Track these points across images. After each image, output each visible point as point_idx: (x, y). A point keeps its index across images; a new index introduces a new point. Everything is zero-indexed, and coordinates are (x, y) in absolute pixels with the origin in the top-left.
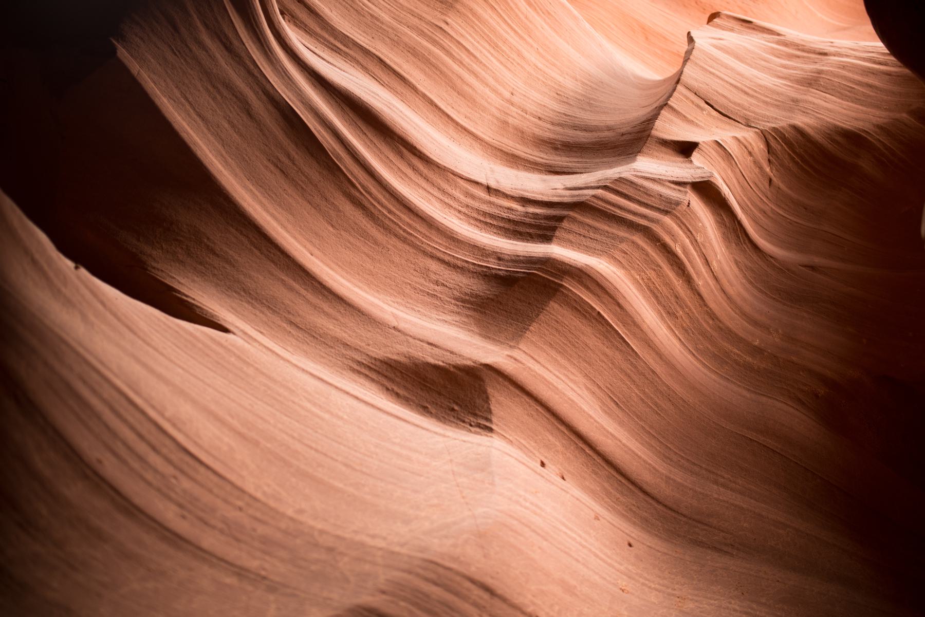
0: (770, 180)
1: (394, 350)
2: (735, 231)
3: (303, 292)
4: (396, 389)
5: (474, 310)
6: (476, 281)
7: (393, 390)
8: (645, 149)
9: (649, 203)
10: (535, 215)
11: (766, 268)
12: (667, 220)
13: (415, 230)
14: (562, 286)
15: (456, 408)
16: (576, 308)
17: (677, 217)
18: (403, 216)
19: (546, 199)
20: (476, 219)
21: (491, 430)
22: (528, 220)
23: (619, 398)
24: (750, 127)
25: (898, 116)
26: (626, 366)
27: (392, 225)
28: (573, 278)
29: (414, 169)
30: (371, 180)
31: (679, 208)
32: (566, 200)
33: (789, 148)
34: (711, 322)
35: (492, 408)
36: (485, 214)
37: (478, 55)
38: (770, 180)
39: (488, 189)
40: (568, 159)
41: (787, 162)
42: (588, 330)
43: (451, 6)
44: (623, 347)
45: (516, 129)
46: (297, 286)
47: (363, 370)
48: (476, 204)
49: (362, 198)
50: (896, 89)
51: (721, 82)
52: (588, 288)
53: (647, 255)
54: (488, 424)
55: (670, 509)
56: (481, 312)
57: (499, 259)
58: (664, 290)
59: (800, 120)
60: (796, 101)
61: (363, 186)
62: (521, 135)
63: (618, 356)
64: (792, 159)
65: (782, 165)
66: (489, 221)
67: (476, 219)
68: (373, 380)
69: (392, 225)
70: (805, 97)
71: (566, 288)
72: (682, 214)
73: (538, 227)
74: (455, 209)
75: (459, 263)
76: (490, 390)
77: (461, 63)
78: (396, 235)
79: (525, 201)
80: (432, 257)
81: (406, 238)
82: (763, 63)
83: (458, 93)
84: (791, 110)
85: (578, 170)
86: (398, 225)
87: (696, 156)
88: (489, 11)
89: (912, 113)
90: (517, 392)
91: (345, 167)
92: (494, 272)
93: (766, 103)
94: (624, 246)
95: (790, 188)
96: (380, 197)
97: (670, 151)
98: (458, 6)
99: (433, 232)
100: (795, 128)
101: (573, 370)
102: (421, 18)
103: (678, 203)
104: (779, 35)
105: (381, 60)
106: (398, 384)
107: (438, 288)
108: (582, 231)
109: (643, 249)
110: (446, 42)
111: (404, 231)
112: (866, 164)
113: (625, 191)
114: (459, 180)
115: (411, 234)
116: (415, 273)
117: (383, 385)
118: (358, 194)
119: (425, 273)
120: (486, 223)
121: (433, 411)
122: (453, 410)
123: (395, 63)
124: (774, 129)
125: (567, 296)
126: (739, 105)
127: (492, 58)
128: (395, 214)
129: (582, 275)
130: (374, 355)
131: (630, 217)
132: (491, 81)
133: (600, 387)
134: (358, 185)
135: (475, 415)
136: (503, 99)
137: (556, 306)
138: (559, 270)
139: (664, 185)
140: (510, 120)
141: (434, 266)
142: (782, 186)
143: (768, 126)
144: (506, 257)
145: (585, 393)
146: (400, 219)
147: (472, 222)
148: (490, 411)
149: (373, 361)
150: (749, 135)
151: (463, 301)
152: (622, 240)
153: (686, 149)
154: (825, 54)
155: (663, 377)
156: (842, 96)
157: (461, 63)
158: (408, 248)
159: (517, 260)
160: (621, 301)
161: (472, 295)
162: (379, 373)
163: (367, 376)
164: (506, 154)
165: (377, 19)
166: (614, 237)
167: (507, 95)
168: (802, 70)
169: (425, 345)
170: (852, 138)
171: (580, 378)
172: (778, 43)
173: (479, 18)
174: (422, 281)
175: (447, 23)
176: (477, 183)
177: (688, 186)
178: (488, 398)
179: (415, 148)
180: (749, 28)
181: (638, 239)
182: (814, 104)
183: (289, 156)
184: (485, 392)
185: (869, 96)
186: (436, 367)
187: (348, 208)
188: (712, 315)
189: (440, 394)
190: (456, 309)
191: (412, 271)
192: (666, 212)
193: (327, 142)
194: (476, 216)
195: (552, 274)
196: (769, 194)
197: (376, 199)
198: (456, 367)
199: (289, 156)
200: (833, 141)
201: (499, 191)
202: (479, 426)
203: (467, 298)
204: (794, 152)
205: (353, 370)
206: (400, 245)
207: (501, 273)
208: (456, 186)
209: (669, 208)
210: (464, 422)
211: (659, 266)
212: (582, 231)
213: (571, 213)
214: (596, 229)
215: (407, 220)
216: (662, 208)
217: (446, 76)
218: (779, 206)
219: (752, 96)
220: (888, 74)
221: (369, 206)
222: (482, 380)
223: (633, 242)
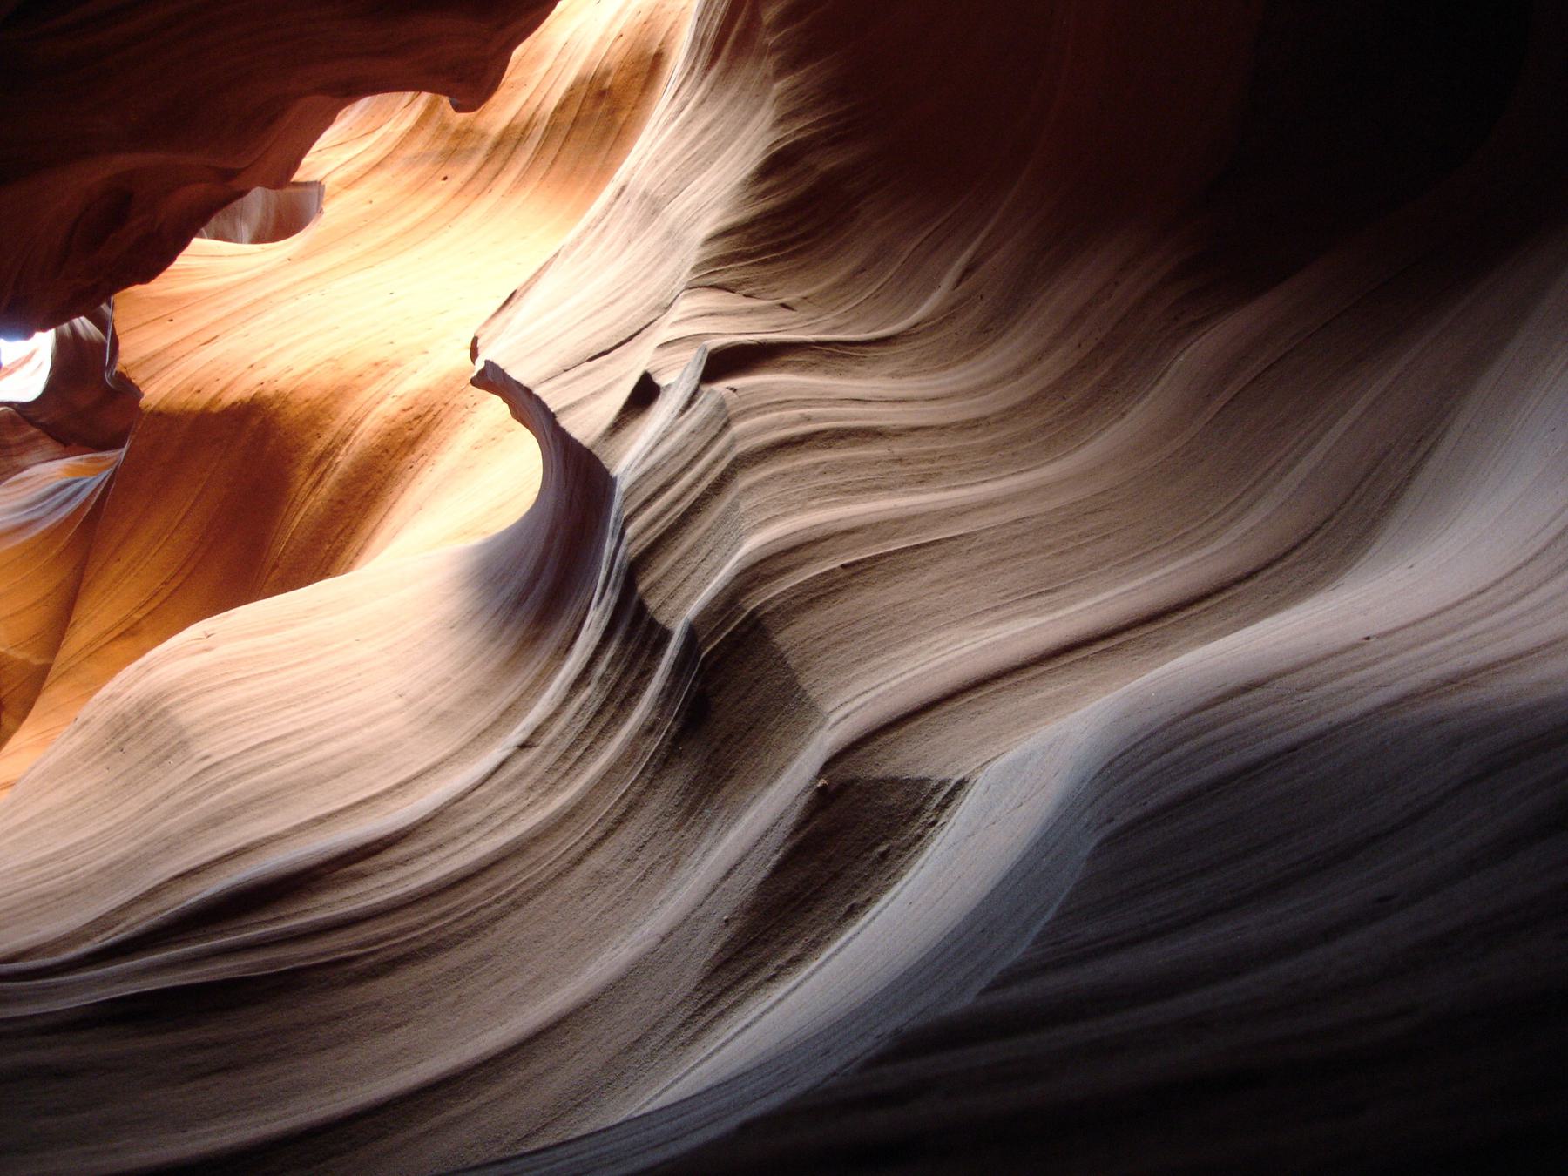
0: (784, 306)
1: (706, 945)
2: (830, 356)
3: (474, 1104)
4: (780, 962)
5: (717, 791)
6: (667, 781)
7: (780, 968)
8: (606, 463)
9: (694, 452)
10: (614, 662)
11: (930, 339)
12: (737, 428)
13: (510, 880)
14: (753, 613)
15: (883, 848)
16: (811, 601)
17: (744, 412)
18: (468, 896)
19: (597, 639)
21: (961, 784)
22: (614, 677)
23: (1036, 587)
25: (772, 96)
26: (980, 558)
27: (471, 920)
28: (750, 590)
29: (404, 862)
31: (729, 404)
33: (741, 260)
34: (979, 431)
35: (917, 776)
36: (563, 758)
37: (296, 727)
38: (784, 306)
41: (765, 272)
42: (868, 595)
43: (184, 743)
44: (936, 552)
45: (463, 700)
46: (453, 1112)
47: (702, 1021)
48: (538, 772)
49: (383, 954)
50: (730, 94)
53: (785, 474)
54: (948, 788)
55: (1305, 540)
56: (728, 779)
58: (874, 472)
60: (669, 233)
62: (481, 693)
63: (952, 564)
64: (764, 263)
65: (768, 281)
66: (578, 753)
68: (736, 1004)
69: (471, 920)
70: (672, 219)
71: (760, 607)
72: (744, 403)
73: (636, 655)
74: (523, 811)
75: (618, 811)
76: (878, 773)
77: (289, 756)
78: (496, 919)
80: (579, 861)
81: (513, 903)
83: (337, 776)
87: (661, 380)
88: (238, 688)
89: (779, 74)
90: (913, 725)
91: (302, 959)
92: (667, 743)
93: (646, 277)
94: (744, 506)
95: (818, 282)
96: (402, 924)
97: (635, 422)
98: (189, 733)
99: (533, 850)
101: (934, 638)
103: (721, 405)
105: (182, 876)
106: (774, 955)
108: (684, 574)
109: (773, 477)
110: (236, 767)
111: (497, 901)
113: (652, 490)
114: (477, 793)
115: (514, 890)
116: (588, 900)
117: (757, 988)
118: (371, 960)
119: (600, 878)
121: (867, 895)
122: (884, 855)
124: (695, 269)
125: (778, 609)
126: (625, 315)
128: (456, 909)
129: (757, 573)
130: (687, 991)
131: (704, 485)
132: (354, 721)
133: (996, 609)
134: (352, 953)
135: (917, 812)
136: (400, 711)
137: (787, 633)
138: (721, 612)
139: (679, 426)
140: (443, 707)
141: (596, 861)
143: (685, 276)
144: (654, 716)
145: (990, 631)
146: (472, 901)
148: (922, 782)
149: (700, 994)
150: (686, 305)
151: (691, 811)
152: (734, 506)
153: (645, 393)
154: (623, 188)
155: (1034, 511)
156: (701, 169)
158: (532, 904)
159: (667, 695)
160: (843, 526)
161: (687, 792)
162: (727, 989)
163: (721, 1014)
164: (496, 723)
165: (110, 866)
166: (724, 519)
167: (398, 703)
169: (725, 885)
170: (774, 166)
171: (955, 633)
172: (566, 256)
173: (236, 707)
174: (610, 888)
175: (206, 757)
177: (705, 388)
178: (894, 780)
179: (366, 846)
181: (744, 480)
183: (202, 1047)
184: (879, 783)
185: (721, 133)
186: (778, 869)
187: (385, 987)
189: (837, 876)
190: (696, 829)
191: (582, 904)
192: (726, 426)
193: (229, 969)
195: (724, 625)
196: (807, 315)
198: (799, 827)
199: (202, 1047)
201: (539, 727)
202: (942, 807)
203: (687, 804)
205: (694, 1039)
206: (515, 918)
207: (674, 730)
209: (724, 420)
210: (920, 837)
211: (817, 465)
212: (684, 574)
213: (641, 588)
214: (693, 549)
215: (481, 889)
218: (839, 306)
219: (624, 294)
220: (702, 102)
221: (407, 949)
222: (856, 780)
223: (749, 489)
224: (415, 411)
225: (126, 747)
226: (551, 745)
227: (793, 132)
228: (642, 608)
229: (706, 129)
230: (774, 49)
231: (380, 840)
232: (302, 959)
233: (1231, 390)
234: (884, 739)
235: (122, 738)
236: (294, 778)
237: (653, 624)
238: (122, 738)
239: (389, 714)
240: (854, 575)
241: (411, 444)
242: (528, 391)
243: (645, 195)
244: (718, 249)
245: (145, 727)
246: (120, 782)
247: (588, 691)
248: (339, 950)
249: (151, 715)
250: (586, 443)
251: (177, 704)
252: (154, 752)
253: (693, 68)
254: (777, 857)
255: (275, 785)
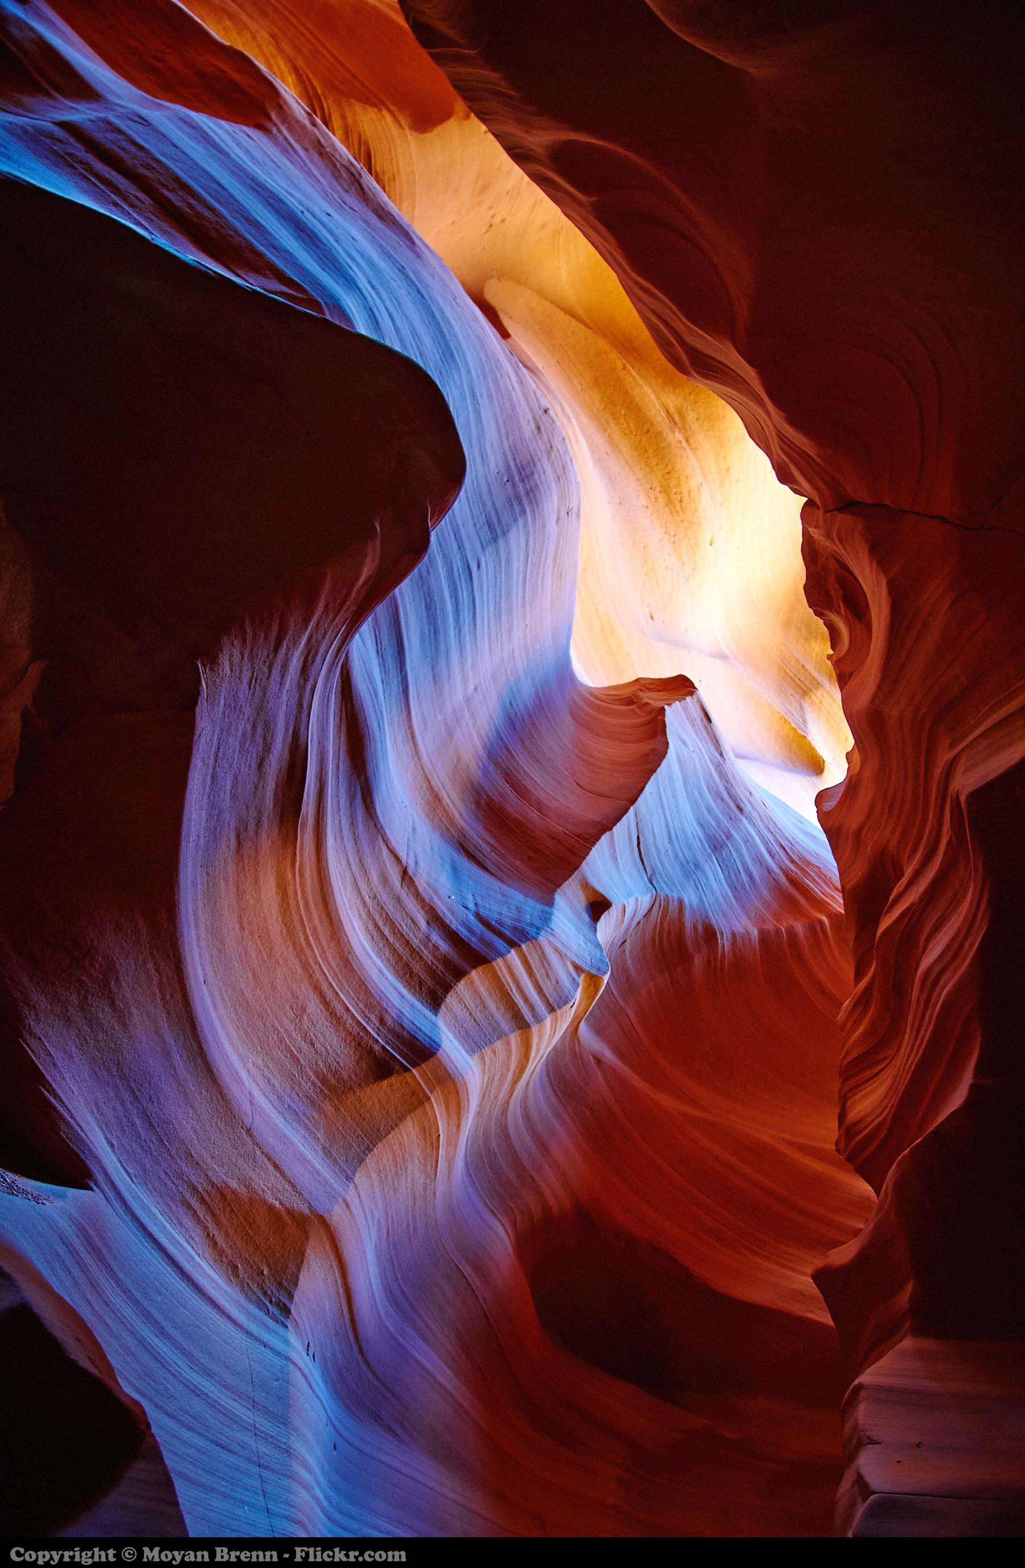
8: (565, 886)
13: (317, 938)
14: (429, 1099)
20: (376, 926)
24: (651, 883)
27: (298, 927)
29: (353, 824)
30: (314, 859)
32: (474, 941)
36: (389, 920)
39: (405, 872)
40: (483, 832)
41: (649, 934)
51: (662, 815)
52: (447, 1107)
57: (382, 1021)
59: (690, 897)
60: (697, 866)
61: (301, 865)
64: (655, 927)
66: (387, 932)
67: (376, 926)
75: (339, 1010)
77: (459, 630)
79: (435, 918)
80: (317, 988)
81: (302, 950)
82: (697, 794)
84: (688, 876)
85: (490, 866)
86: (304, 926)
89: (761, 932)
93: (676, 855)
95: (631, 953)
98: (501, 542)
100: (681, 902)
102: (461, 547)
104: (721, 755)
107: (304, 1046)
112: (698, 961)
115: (310, 946)
120: (383, 935)
123: (406, 614)
127: (486, 630)
139: (565, 966)
140: (458, 734)
141: (314, 1006)
142: (627, 951)
146: (310, 919)
147: (371, 926)
148: (295, 1282)
151: (324, 1081)
154: (741, 810)
157: (460, 631)
168: (718, 823)
169: (271, 1167)
174: (292, 1028)
176: (397, 859)
178: (302, 1261)
180: (706, 727)
182: (707, 879)
184: (302, 1254)
188: (504, 1112)
194: (377, 917)
197: (302, 884)
198: (290, 1212)
200: (695, 927)
204: (661, 923)
207: (376, 1047)
208: (378, 857)
216: (551, 1000)
217: (437, 649)
220: (769, 871)
224: (686, 500)
225: (509, 485)
226: (399, 900)
227: (724, 942)
228: (459, 974)
229: (751, 877)
230: (778, 931)
231: (372, 802)
232: (302, 841)
233: (467, 1270)
234: (327, 1243)
235: (517, 478)
236: (442, 646)
237: (448, 988)
238: (517, 478)
239: (466, 688)
240: (432, 1143)
241: (666, 490)
242: (633, 801)
243: (729, 837)
244: (673, 908)
245: (518, 498)
246: (485, 489)
247: (423, 923)
248: (302, 855)
249: (525, 501)
250: (584, 864)
251: (526, 526)
252: (497, 514)
253: (792, 861)
254: (277, 1205)
255: (441, 639)
